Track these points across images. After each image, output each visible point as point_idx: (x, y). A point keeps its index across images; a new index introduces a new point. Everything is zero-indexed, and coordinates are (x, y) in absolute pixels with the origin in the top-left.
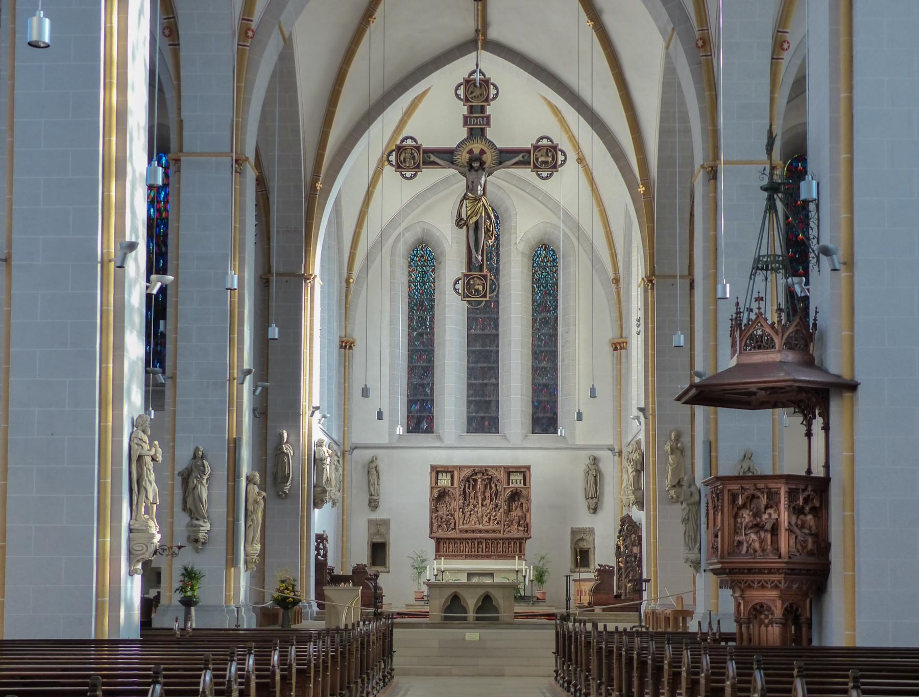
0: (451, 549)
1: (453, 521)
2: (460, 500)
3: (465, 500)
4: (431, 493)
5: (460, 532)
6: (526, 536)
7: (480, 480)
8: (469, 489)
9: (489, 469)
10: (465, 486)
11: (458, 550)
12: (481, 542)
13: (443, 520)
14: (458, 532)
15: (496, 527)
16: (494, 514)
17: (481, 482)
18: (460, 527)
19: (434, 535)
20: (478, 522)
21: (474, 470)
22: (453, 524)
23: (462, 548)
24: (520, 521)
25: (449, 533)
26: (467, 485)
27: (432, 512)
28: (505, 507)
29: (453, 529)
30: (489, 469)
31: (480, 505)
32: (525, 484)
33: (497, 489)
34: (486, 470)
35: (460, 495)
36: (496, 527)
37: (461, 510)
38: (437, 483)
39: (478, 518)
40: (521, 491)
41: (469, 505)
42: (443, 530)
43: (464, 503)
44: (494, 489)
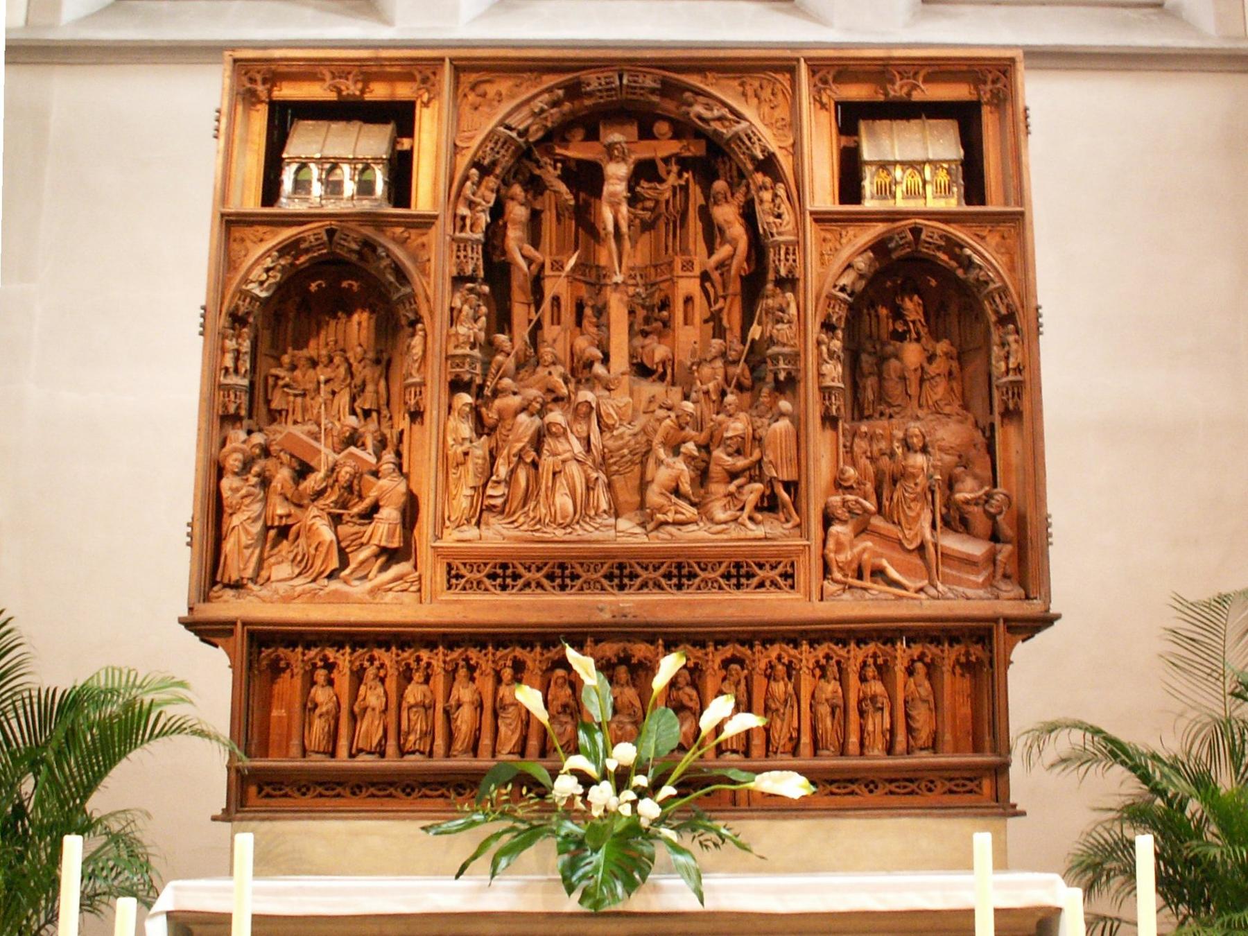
0: (371, 730)
1: (390, 488)
2: (454, 316)
3: (502, 321)
4: (227, 261)
5: (453, 576)
6: (1009, 604)
7: (617, 174)
8: (535, 241)
9: (694, 80)
10: (498, 211)
11: (429, 734)
12: (625, 660)
13: (312, 482)
14: (433, 572)
15: (759, 531)
16: (737, 426)
17: (633, 181)
18: (451, 538)
19: (228, 607)
20: (602, 499)
21: (574, 90)
22: (389, 514)
23: (464, 719)
24: (951, 483)
25: (359, 589)
26: (517, 212)
27: (229, 419)
28: (834, 372)
29: (390, 556)
30: (694, 80)
31: (620, 362)
32: (974, 188)
33: (758, 246)
34: (669, 89)
35: (459, 280)
36: (759, 531)
37: (466, 398)
38: (271, 192)
39: (603, 463)
40: (953, 246)
41: (529, 362)
42: (304, 565)
43: (490, 347)
44: (737, 230)
